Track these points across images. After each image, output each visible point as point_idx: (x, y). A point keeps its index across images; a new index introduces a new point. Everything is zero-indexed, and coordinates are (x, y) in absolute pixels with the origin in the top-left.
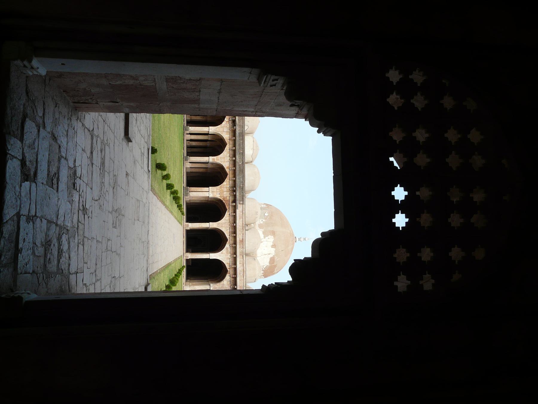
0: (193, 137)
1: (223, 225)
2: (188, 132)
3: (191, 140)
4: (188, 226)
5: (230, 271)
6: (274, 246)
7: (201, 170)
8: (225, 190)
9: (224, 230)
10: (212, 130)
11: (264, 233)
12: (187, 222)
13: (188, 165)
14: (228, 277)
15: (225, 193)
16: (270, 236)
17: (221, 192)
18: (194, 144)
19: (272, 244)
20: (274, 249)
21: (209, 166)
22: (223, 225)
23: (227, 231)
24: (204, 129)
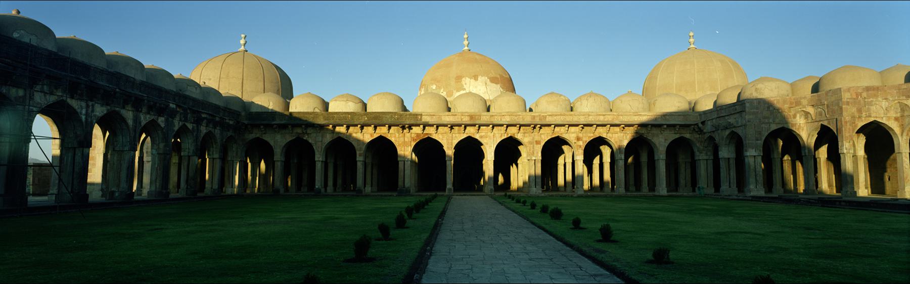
0: (330, 183)
1: (449, 142)
2: (323, 190)
3: (335, 184)
4: (450, 189)
5: (512, 131)
6: (476, 78)
7: (375, 172)
8: (402, 139)
9: (455, 142)
10: (319, 157)
11: (458, 91)
12: (444, 190)
13: (368, 189)
14: (519, 137)
15: (406, 140)
16: (463, 83)
17: (405, 144)
18: (339, 182)
19: (472, 80)
20: (480, 78)
21: (369, 161)
22: (449, 142)
23: (459, 136)
24: (319, 166)
